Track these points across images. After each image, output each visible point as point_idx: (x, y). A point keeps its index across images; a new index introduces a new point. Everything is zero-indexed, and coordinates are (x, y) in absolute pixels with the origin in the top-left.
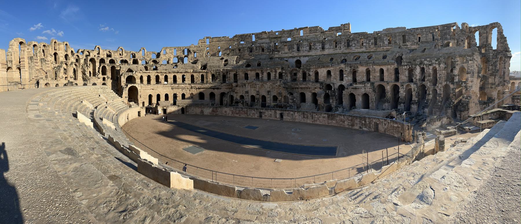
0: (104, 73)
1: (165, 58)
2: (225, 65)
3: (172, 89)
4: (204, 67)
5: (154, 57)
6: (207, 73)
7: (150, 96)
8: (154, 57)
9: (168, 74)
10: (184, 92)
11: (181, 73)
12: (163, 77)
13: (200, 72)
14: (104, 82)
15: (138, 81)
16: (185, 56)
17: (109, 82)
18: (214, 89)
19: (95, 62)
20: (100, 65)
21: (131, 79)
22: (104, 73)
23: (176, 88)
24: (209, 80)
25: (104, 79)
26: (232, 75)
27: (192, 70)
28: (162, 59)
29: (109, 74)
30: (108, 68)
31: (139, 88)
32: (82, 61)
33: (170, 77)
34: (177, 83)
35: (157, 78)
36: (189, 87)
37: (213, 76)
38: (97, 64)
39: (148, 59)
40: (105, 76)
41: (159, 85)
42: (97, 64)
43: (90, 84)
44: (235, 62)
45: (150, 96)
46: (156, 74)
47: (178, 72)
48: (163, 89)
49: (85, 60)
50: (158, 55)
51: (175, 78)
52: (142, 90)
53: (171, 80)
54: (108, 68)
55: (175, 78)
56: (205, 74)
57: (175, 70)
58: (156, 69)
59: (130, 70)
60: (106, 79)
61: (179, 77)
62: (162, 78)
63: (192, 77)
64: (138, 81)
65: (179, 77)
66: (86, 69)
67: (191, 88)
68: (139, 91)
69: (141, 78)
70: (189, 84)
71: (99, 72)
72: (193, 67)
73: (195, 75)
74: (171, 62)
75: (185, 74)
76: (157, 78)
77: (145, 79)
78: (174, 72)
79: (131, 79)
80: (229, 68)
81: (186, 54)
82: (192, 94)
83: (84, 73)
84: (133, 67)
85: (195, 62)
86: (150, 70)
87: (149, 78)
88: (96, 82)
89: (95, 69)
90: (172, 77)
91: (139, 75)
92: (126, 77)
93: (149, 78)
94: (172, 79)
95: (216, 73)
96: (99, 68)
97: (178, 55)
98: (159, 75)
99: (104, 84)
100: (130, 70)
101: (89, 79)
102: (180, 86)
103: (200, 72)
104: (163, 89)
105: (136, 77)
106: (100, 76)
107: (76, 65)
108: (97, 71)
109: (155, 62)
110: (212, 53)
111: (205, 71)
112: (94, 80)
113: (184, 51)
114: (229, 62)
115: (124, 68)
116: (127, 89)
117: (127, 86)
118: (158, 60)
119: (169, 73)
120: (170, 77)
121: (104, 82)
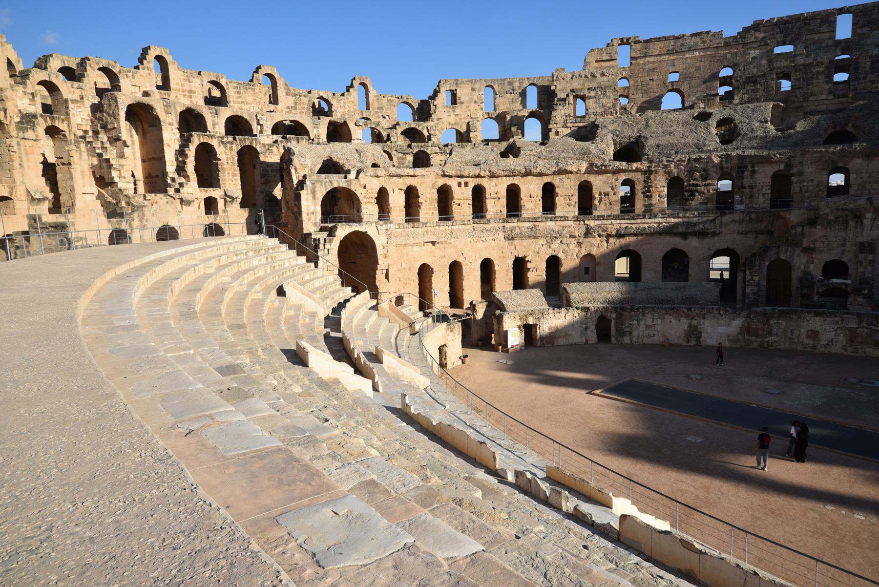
0: (208, 174)
1: (452, 119)
2: (725, 140)
3: (510, 238)
4: (629, 152)
5: (407, 119)
6: (648, 173)
7: (425, 272)
8: (407, 119)
9: (484, 182)
10: (557, 249)
11: (540, 174)
12: (468, 192)
13: (617, 171)
14: (210, 219)
15: (370, 209)
16: (532, 115)
17: (235, 216)
18: (684, 235)
19: (156, 123)
20: (185, 142)
21: (339, 205)
22: (208, 174)
23: (522, 236)
24: (655, 199)
25: (210, 205)
26: (764, 177)
27: (584, 166)
28: (442, 125)
29: (231, 181)
30: (227, 156)
31: (380, 241)
32: (80, 117)
33: (496, 191)
34: (525, 214)
35: (444, 196)
36: (578, 229)
37: (674, 184)
38: (171, 136)
39: (386, 123)
40: (216, 193)
41: (446, 227)
42: (171, 136)
43: (142, 231)
44: (771, 127)
45: (425, 272)
46: (441, 182)
47: (528, 174)
48: (471, 243)
49: (96, 109)
50: (423, 111)
51: (513, 193)
52: (392, 249)
53: (496, 205)
54: (227, 156)
55: (513, 193)
56: (638, 178)
57: (511, 162)
58: (422, 160)
59: (330, 167)
60: (221, 203)
61: (531, 192)
62: (462, 196)
63: (585, 190)
64: (370, 209)
65: (531, 192)
66: (111, 154)
67: (588, 233)
68: (380, 252)
69: (382, 197)
70: (576, 220)
71: (181, 169)
72: (585, 153)
73: (598, 183)
74: (477, 136)
75: (556, 180)
76: (444, 196)
77: (397, 200)
78: (512, 174)
79: (339, 205)
80: (748, 152)
81: (533, 103)
82: (589, 256)
83: (103, 180)
84: (338, 151)
85: (586, 133)
86: (401, 164)
87: (411, 194)
88: (173, 223)
89: (161, 160)
90: (503, 193)
91: (374, 186)
92: (321, 194)
93: (411, 194)
94: (504, 201)
95: (691, 171)
96: (181, 153)
97: (501, 109)
98: (453, 183)
99: (214, 231)
100: (330, 167)
101: (134, 208)
102: (541, 225)
103: (617, 171)
104: (471, 243)
105: (360, 192)
106: (192, 189)
107: (52, 132)
108: (171, 168)
109: (412, 134)
110: (640, 98)
111: (643, 165)
112: (161, 210)
113: (523, 94)
114: (744, 128)
115: (306, 158)
116: (334, 245)
117: (331, 232)
118: (423, 127)
119: (493, 176)
120: (496, 191)
121: (210, 219)
